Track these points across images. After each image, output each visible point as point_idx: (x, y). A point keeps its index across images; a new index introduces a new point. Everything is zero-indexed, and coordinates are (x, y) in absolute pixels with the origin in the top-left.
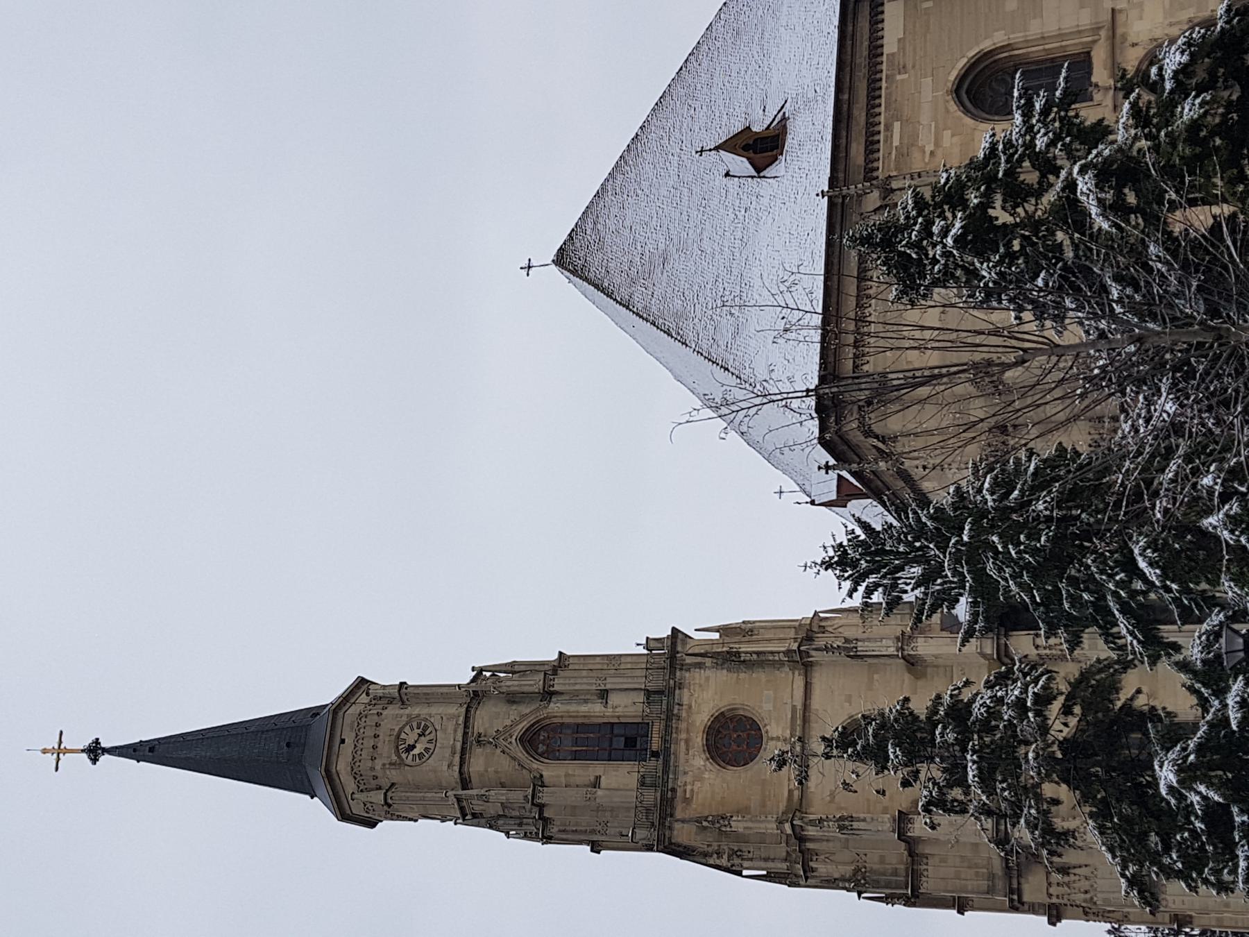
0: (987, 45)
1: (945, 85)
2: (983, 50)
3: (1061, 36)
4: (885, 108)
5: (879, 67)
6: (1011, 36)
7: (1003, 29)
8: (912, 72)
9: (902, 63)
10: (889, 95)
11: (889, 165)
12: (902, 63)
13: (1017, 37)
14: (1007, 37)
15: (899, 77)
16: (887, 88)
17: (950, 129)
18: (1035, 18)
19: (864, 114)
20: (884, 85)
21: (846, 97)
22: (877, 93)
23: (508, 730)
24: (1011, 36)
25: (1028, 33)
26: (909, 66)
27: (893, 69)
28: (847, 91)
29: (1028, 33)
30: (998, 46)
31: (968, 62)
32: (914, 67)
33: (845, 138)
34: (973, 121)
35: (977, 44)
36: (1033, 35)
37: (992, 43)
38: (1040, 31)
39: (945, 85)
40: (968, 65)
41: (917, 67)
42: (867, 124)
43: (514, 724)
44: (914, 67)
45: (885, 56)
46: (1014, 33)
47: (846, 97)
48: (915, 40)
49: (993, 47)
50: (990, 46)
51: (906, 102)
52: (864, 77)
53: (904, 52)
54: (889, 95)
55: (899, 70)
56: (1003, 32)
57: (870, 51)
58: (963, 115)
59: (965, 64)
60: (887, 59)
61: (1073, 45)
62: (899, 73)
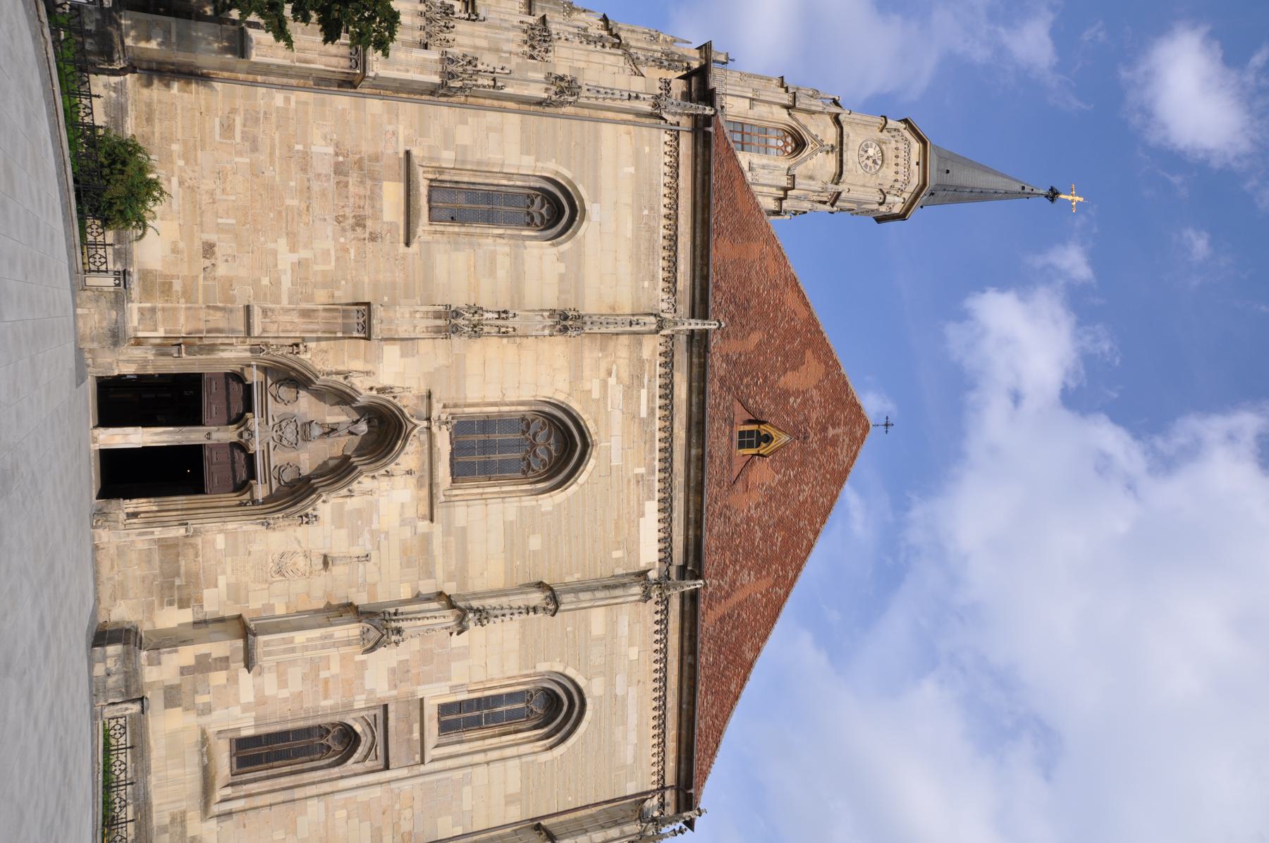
0: (559, 496)
1: (598, 454)
2: (562, 491)
3: (483, 498)
4: (654, 437)
5: (662, 486)
6: (534, 503)
7: (543, 514)
8: (630, 474)
9: (641, 486)
10: (652, 451)
11: (650, 366)
12: (641, 486)
13: (529, 501)
14: (540, 502)
15: (642, 470)
16: (654, 459)
17: (593, 400)
18: (512, 522)
19: (675, 431)
20: (657, 463)
21: (694, 452)
22: (663, 455)
23: (814, 153)
24: (534, 503)
25: (518, 504)
26: (633, 482)
27: (648, 480)
28: (693, 459)
29: (518, 504)
30: (548, 494)
31: (577, 479)
32: (629, 481)
33: (694, 403)
34: (570, 405)
35: (568, 499)
36: (513, 502)
37: (554, 498)
38: (506, 505)
39: (598, 454)
40: (577, 475)
41: (625, 480)
42: (672, 419)
43: (811, 156)
44: (629, 481)
45: (657, 499)
46: (533, 507)
47: (694, 452)
48: (629, 513)
49: (552, 493)
50: (554, 495)
51: (635, 440)
52: (676, 475)
53: (639, 500)
54: (652, 451)
55: (643, 480)
56: (543, 510)
57: (671, 506)
58: (581, 414)
59: (579, 476)
60: (654, 496)
61: (470, 490)
62: (643, 475)
